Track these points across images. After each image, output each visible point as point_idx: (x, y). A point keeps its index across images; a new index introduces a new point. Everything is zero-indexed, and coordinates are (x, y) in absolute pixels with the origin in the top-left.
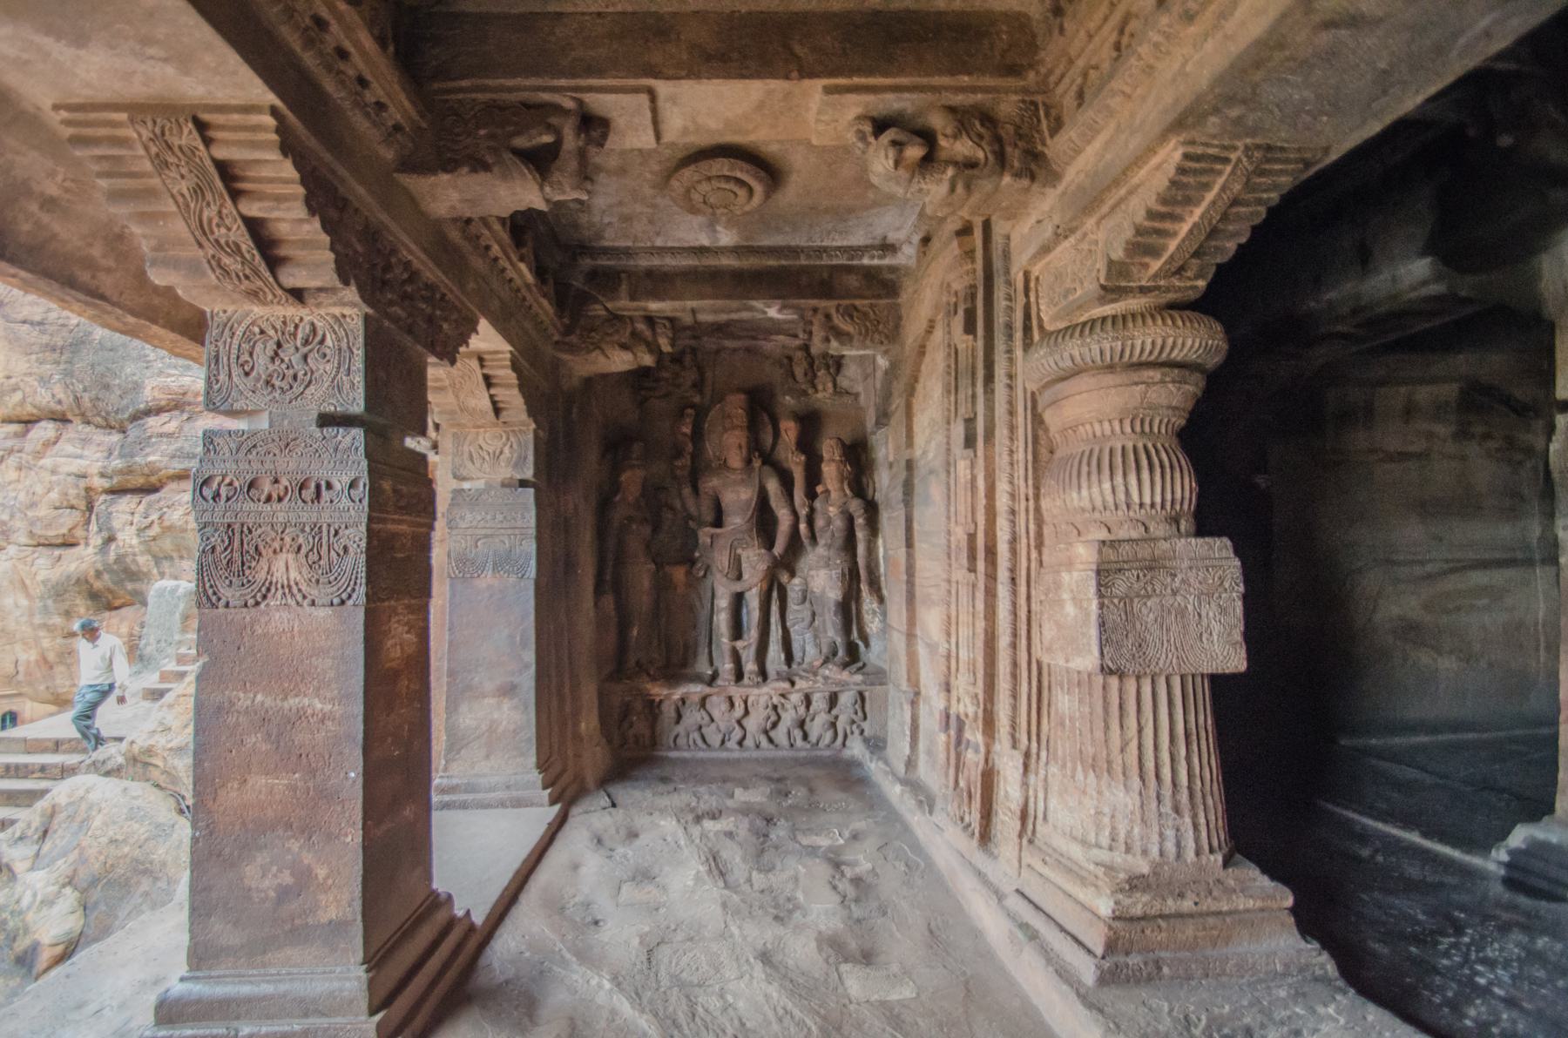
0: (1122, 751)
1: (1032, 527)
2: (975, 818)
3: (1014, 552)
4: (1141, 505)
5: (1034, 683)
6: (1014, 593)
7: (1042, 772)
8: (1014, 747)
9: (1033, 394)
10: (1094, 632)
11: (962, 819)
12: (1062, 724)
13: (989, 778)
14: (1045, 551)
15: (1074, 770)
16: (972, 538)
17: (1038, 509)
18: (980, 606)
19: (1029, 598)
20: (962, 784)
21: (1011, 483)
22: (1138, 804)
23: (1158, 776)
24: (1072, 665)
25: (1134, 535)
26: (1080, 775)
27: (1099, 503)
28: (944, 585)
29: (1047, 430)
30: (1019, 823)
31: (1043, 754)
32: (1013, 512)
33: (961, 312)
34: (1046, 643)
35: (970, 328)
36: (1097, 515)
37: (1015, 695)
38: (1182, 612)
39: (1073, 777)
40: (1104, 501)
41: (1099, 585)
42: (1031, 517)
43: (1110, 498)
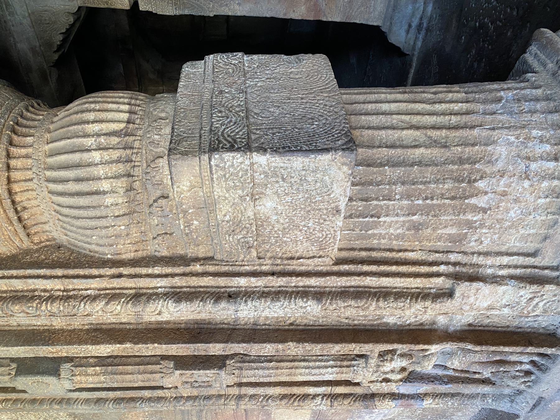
0: (445, 147)
1: (157, 270)
2: (521, 356)
4: (128, 122)
5: (366, 268)
6: (248, 295)
7: (475, 259)
8: (450, 294)
10: (298, 162)
11: (528, 373)
12: (416, 227)
13: (478, 335)
14: (191, 252)
15: (475, 209)
16: (182, 363)
17: (134, 263)
18: (269, 349)
19: (254, 274)
20: (487, 373)
22: (505, 132)
23: (467, 113)
24: (342, 206)
25: (168, 130)
26: (481, 201)
27: (120, 168)
28: (244, 405)
29: (27, 252)
30: (548, 287)
31: (453, 257)
32: (138, 297)
34: (314, 250)
36: (137, 172)
37: (383, 294)
38: (268, 89)
39: (484, 211)
40: (118, 161)
41: (232, 148)
42: (144, 271)
43: (115, 154)
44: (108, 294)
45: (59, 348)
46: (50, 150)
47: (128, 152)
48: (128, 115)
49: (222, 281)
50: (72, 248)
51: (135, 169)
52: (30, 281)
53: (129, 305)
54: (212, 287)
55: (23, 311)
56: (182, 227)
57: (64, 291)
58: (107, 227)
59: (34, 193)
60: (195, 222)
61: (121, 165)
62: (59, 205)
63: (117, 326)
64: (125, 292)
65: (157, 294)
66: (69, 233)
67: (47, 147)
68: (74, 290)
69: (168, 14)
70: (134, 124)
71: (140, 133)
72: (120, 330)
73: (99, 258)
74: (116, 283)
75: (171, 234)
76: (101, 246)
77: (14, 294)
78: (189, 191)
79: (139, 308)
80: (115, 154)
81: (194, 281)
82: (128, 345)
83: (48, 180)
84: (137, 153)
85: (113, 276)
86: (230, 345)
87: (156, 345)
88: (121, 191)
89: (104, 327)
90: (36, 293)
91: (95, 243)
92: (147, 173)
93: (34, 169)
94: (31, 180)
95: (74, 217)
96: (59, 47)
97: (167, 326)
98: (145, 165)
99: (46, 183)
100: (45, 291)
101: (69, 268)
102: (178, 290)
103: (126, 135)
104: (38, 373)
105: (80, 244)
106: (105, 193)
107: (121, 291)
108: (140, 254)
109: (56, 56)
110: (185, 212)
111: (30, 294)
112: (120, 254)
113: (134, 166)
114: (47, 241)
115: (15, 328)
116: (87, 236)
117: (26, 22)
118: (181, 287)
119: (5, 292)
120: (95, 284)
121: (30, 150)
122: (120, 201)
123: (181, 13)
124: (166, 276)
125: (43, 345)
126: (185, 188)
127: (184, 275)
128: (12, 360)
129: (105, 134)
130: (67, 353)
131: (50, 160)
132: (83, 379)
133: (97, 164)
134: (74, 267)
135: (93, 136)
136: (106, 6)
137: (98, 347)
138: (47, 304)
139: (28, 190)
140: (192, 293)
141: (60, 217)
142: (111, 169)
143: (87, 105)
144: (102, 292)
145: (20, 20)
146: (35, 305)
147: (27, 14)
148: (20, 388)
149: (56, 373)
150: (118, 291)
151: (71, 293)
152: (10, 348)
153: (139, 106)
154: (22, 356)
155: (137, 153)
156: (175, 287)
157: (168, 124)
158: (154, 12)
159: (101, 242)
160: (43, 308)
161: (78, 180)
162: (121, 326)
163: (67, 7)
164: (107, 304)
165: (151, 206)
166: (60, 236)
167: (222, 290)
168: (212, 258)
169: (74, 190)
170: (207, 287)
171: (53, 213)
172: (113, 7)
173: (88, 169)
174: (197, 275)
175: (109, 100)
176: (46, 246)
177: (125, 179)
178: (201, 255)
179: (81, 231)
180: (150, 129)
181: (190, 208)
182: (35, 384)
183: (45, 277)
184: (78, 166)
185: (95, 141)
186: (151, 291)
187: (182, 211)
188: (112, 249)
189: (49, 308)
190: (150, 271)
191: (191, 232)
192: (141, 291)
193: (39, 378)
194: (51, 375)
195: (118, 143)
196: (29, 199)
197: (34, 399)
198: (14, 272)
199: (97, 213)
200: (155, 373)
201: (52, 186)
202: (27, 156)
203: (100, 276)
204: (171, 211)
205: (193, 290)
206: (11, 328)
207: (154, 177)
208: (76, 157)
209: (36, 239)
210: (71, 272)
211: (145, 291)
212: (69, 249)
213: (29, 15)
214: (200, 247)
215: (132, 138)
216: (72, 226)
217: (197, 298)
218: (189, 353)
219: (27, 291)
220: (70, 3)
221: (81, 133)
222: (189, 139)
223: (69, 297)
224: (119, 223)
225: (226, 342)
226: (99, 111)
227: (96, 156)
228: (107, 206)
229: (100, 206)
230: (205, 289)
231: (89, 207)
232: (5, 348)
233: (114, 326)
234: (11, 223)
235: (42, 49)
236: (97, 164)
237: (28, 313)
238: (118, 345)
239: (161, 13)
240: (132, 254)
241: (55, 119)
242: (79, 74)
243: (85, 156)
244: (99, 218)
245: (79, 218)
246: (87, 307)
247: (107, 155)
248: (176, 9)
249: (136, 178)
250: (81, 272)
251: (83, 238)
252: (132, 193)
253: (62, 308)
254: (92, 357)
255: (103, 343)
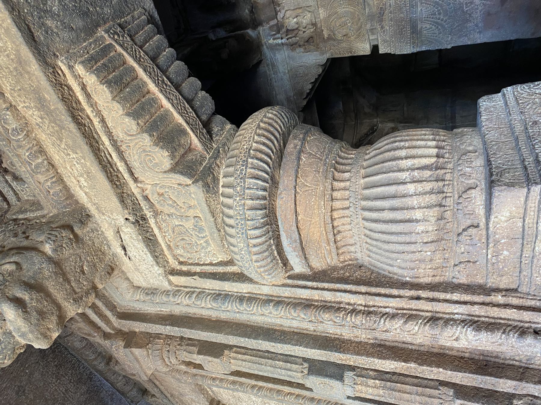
1: (456, 296)
3: (491, 326)
4: (438, 156)
9: (290, 277)
14: (491, 282)
21: (394, 316)
25: (479, 162)
27: (434, 199)
29: (334, 269)
33: (198, 359)
35: (214, 350)
36: (449, 202)
40: (431, 192)
42: (442, 296)
43: (428, 186)
44: (405, 314)
45: (349, 356)
46: (366, 183)
47: (441, 184)
48: (437, 150)
49: (527, 316)
50: (372, 268)
51: (447, 199)
52: (338, 294)
53: (427, 327)
54: (514, 320)
55: (331, 320)
56: (489, 256)
57: (365, 306)
58: (414, 252)
59: (349, 219)
60: (505, 253)
61: (433, 197)
62: (370, 230)
63: (400, 345)
64: (421, 313)
65: (453, 320)
66: (372, 254)
67: (362, 181)
68: (374, 306)
69: (405, 53)
70: (444, 158)
71: (450, 166)
72: (402, 349)
73: (397, 279)
74: (414, 304)
75: (475, 262)
76: (403, 269)
77: (324, 304)
78: (506, 221)
79: (437, 331)
80: (428, 186)
81: (495, 312)
82: (413, 365)
83: (364, 209)
84: (448, 185)
85: (412, 298)
86: (524, 384)
87: (441, 370)
88: (433, 220)
89: (387, 343)
90: (342, 306)
91: (398, 267)
92: (458, 203)
93: (351, 200)
94: (348, 208)
95: (384, 242)
96: (308, 94)
97: (450, 353)
98: (456, 196)
99: (362, 212)
100: (349, 304)
101: (372, 286)
102: (476, 319)
103: (437, 168)
104: (327, 376)
105: (380, 265)
106: (417, 221)
107: (418, 313)
108: (437, 279)
109: (305, 103)
110: (497, 242)
111: (337, 306)
112: (418, 277)
113: (446, 197)
114: (350, 260)
115: (311, 333)
116: (392, 259)
117: (286, 77)
118: (479, 316)
119: (317, 301)
120: (393, 303)
121: (348, 183)
122: (430, 229)
123: (418, 49)
124: (465, 303)
125: (336, 351)
126: (503, 219)
127: (483, 304)
128: (305, 360)
129: (417, 169)
130: (354, 362)
131: (367, 192)
132: (364, 388)
133: (412, 195)
134: (377, 286)
135: (407, 170)
136: (350, 55)
137: (384, 362)
138: (351, 316)
139: (344, 217)
140: (491, 324)
141: (369, 241)
142: (424, 199)
143: (397, 144)
144: (399, 312)
145: (282, 76)
146: (341, 316)
147: (287, 71)
148: (308, 385)
149: (340, 378)
150: (414, 312)
151: (372, 309)
152: (309, 350)
153: (444, 141)
154: (316, 358)
155: (448, 185)
156: (473, 316)
157: (478, 157)
158: (392, 53)
159: (403, 265)
160: (348, 319)
161: (393, 209)
162: (404, 346)
163: (318, 61)
164: (405, 322)
165: (459, 235)
166: (363, 257)
167: (527, 325)
168: (516, 290)
169: (388, 218)
170: (508, 320)
171: (363, 237)
172: (355, 55)
173: (404, 200)
174: (498, 305)
175: (415, 138)
176: (349, 265)
177: (437, 208)
178: (502, 286)
179: (387, 254)
180: (460, 162)
181: (503, 238)
182: (322, 385)
183: (350, 292)
184: (394, 197)
185: (410, 175)
186: (447, 316)
187: (494, 241)
188: (411, 273)
189: (353, 320)
190: (448, 296)
191: (498, 262)
192: (438, 315)
193: (327, 380)
194: (338, 379)
195: (430, 176)
196: (343, 225)
197: (313, 398)
198: (326, 285)
199: (407, 239)
200: (434, 398)
201: (367, 214)
202: (345, 189)
203: (400, 297)
204: (480, 240)
205: (493, 321)
206: (308, 332)
207: (466, 207)
208: (392, 189)
209: (342, 258)
210: (373, 290)
211: (441, 315)
212: (369, 269)
213: (288, 71)
214: (504, 278)
215: (443, 171)
216: (380, 249)
217: (498, 329)
218: (474, 384)
219: (334, 302)
220: (321, 57)
221: (395, 168)
222: (511, 171)
223: (370, 313)
224: (425, 249)
225: (520, 380)
226: (408, 148)
227: (411, 188)
228: (418, 233)
229: (411, 233)
230: (506, 322)
231: (401, 233)
232: (305, 349)
233: (397, 344)
234: (329, 244)
235: (295, 97)
236: (412, 195)
237: (335, 322)
238: (403, 364)
239: (399, 53)
240: (430, 279)
241: (367, 157)
242: (316, 115)
243: (401, 189)
244: (408, 243)
245: (389, 243)
246: (386, 323)
247: (420, 187)
248: (413, 47)
249: (448, 208)
250: (383, 291)
251: (386, 260)
252: (442, 222)
253: (364, 322)
254: (372, 370)
255: (388, 359)
